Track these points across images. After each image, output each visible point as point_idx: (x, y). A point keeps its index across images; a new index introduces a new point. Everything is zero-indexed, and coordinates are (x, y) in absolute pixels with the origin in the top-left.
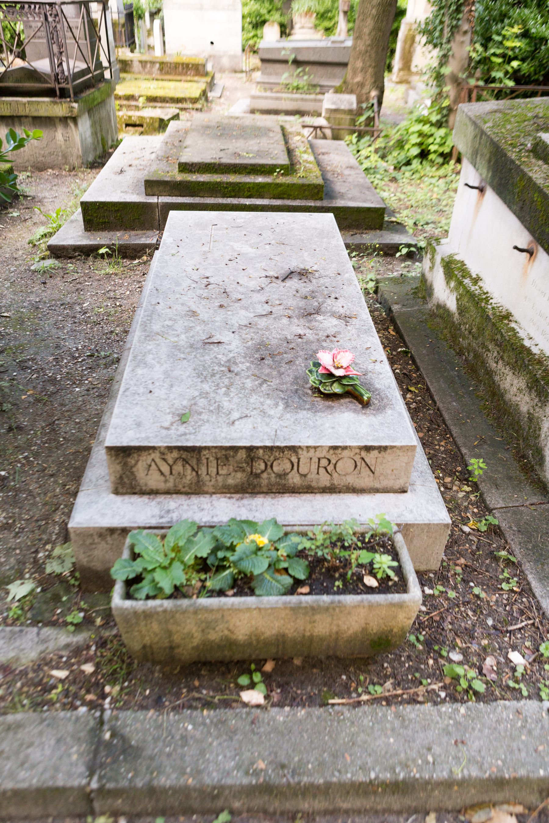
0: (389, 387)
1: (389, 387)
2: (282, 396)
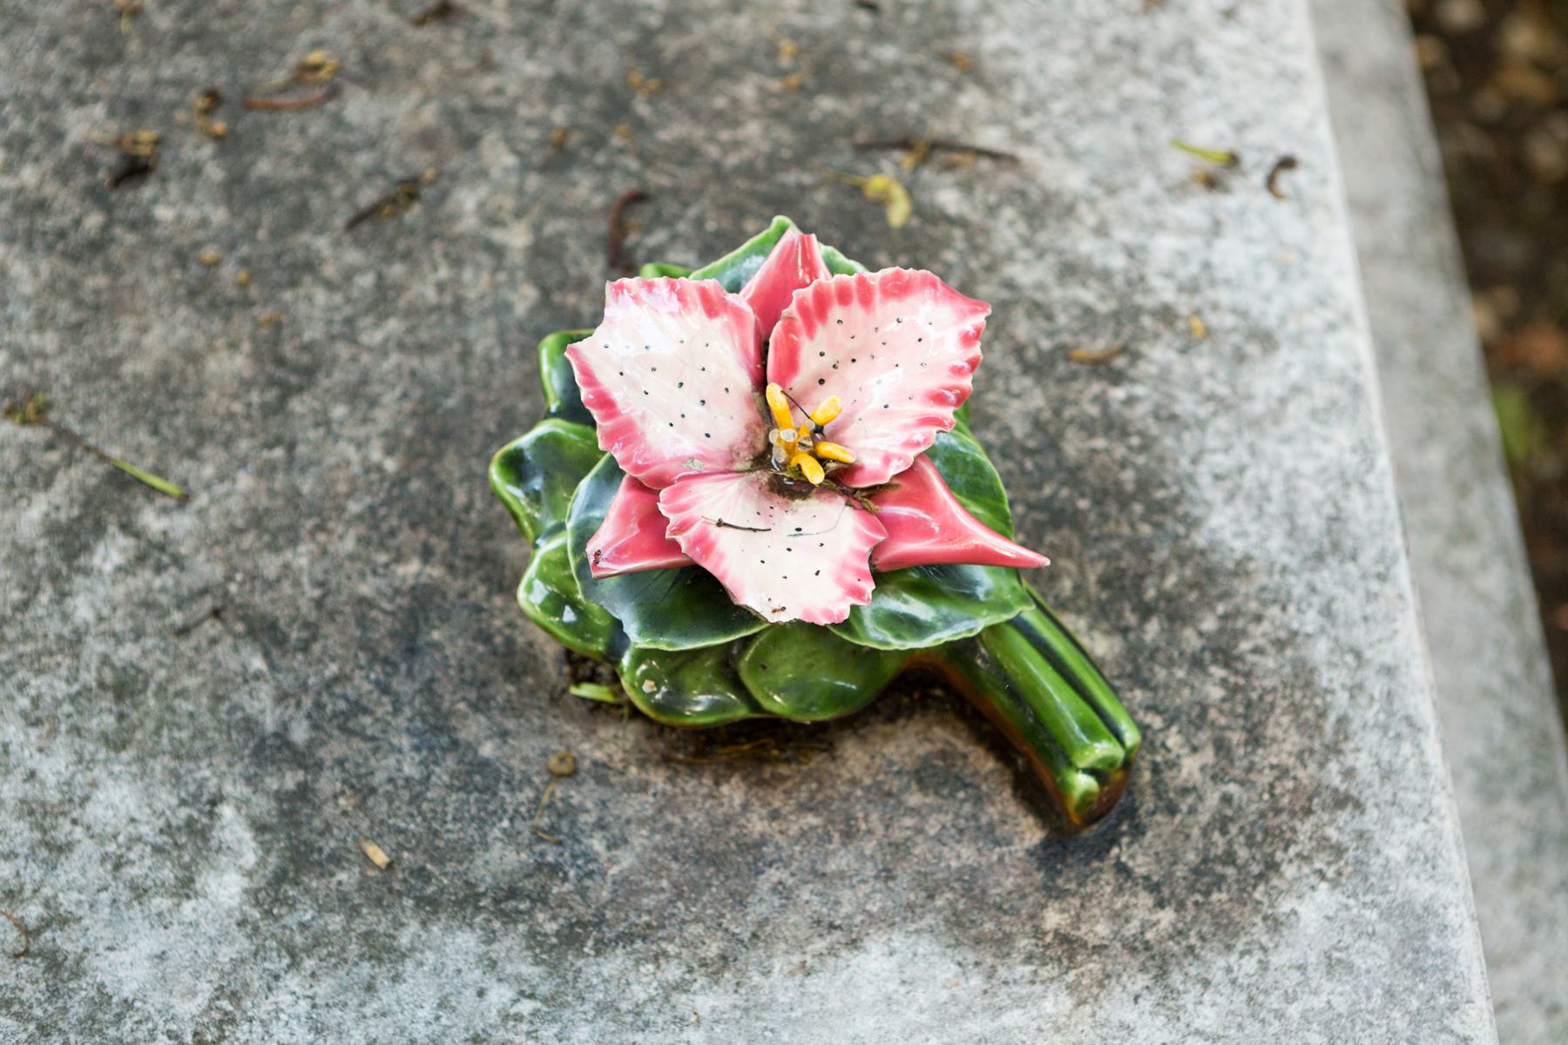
0: (1332, 545)
1: (1332, 545)
2: (262, 706)
